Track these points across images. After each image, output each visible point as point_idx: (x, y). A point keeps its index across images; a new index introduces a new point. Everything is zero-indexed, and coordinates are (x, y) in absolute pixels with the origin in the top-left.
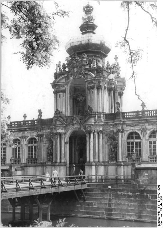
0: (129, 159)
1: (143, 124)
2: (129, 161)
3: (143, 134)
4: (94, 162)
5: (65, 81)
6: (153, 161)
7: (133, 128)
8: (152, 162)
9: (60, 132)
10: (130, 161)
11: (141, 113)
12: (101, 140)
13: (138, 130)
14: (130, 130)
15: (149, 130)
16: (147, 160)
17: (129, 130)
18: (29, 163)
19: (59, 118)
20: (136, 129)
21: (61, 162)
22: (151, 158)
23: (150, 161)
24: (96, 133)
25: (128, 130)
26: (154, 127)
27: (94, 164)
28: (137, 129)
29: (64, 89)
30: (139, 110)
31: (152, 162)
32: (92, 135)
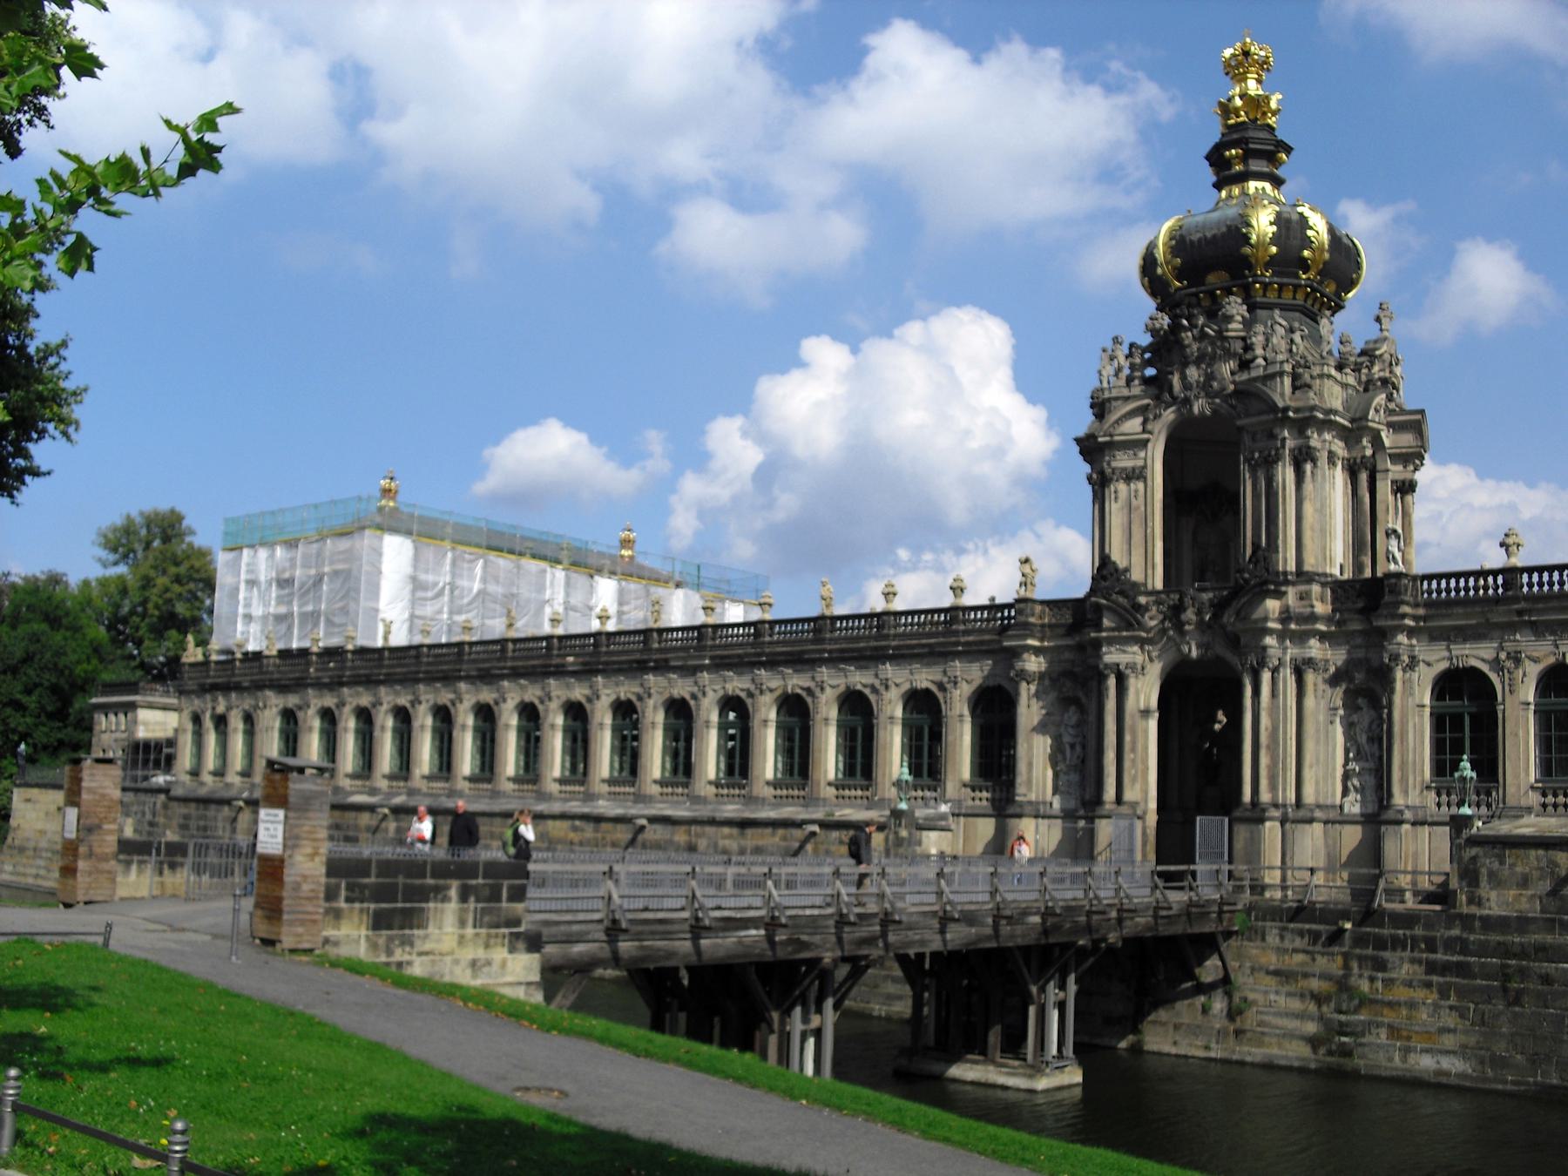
2: (1439, 805)
3: (1507, 681)
4: (1276, 806)
5: (1140, 429)
8: (1550, 808)
9: (1118, 665)
11: (1500, 580)
12: (1309, 702)
15: (1535, 660)
16: (1523, 803)
18: (973, 799)
19: (1114, 596)
20: (1478, 658)
21: (1119, 800)
22: (1544, 795)
23: (1538, 808)
27: (1276, 813)
29: (1140, 463)
30: (1488, 566)
31: (1550, 808)
32: (1266, 676)
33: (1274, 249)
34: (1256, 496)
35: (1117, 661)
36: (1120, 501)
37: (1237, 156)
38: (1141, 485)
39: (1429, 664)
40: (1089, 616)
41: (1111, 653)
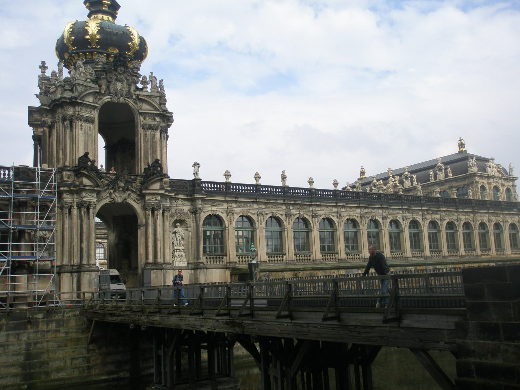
0: (207, 258)
1: (230, 204)
3: (229, 220)
5: (92, 102)
6: (325, 259)
7: (214, 208)
8: (241, 262)
9: (90, 202)
10: (209, 261)
12: (167, 224)
13: (223, 213)
14: (209, 211)
15: (237, 214)
16: (235, 261)
17: (208, 211)
24: (161, 211)
25: (207, 210)
26: (245, 211)
28: (221, 210)
31: (241, 262)
33: (138, 48)
34: (146, 142)
35: (90, 201)
36: (83, 130)
37: (107, 4)
38: (92, 126)
39: (204, 212)
40: (65, 179)
41: (86, 197)
